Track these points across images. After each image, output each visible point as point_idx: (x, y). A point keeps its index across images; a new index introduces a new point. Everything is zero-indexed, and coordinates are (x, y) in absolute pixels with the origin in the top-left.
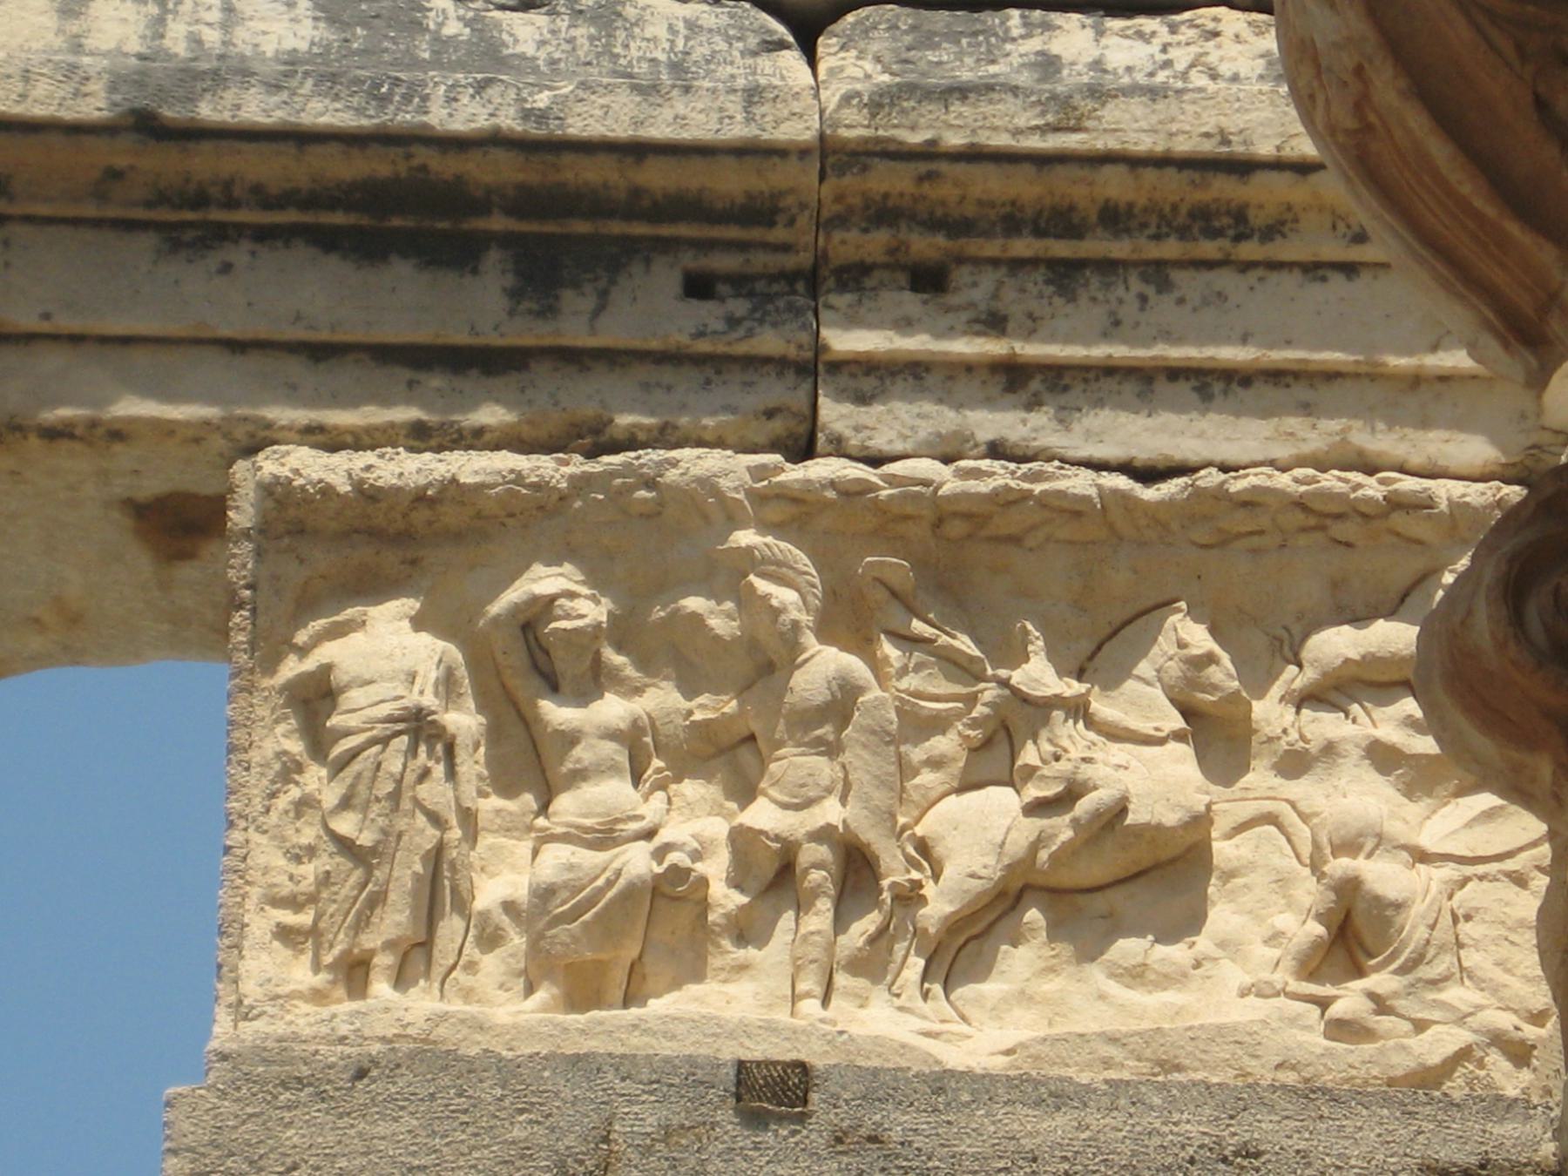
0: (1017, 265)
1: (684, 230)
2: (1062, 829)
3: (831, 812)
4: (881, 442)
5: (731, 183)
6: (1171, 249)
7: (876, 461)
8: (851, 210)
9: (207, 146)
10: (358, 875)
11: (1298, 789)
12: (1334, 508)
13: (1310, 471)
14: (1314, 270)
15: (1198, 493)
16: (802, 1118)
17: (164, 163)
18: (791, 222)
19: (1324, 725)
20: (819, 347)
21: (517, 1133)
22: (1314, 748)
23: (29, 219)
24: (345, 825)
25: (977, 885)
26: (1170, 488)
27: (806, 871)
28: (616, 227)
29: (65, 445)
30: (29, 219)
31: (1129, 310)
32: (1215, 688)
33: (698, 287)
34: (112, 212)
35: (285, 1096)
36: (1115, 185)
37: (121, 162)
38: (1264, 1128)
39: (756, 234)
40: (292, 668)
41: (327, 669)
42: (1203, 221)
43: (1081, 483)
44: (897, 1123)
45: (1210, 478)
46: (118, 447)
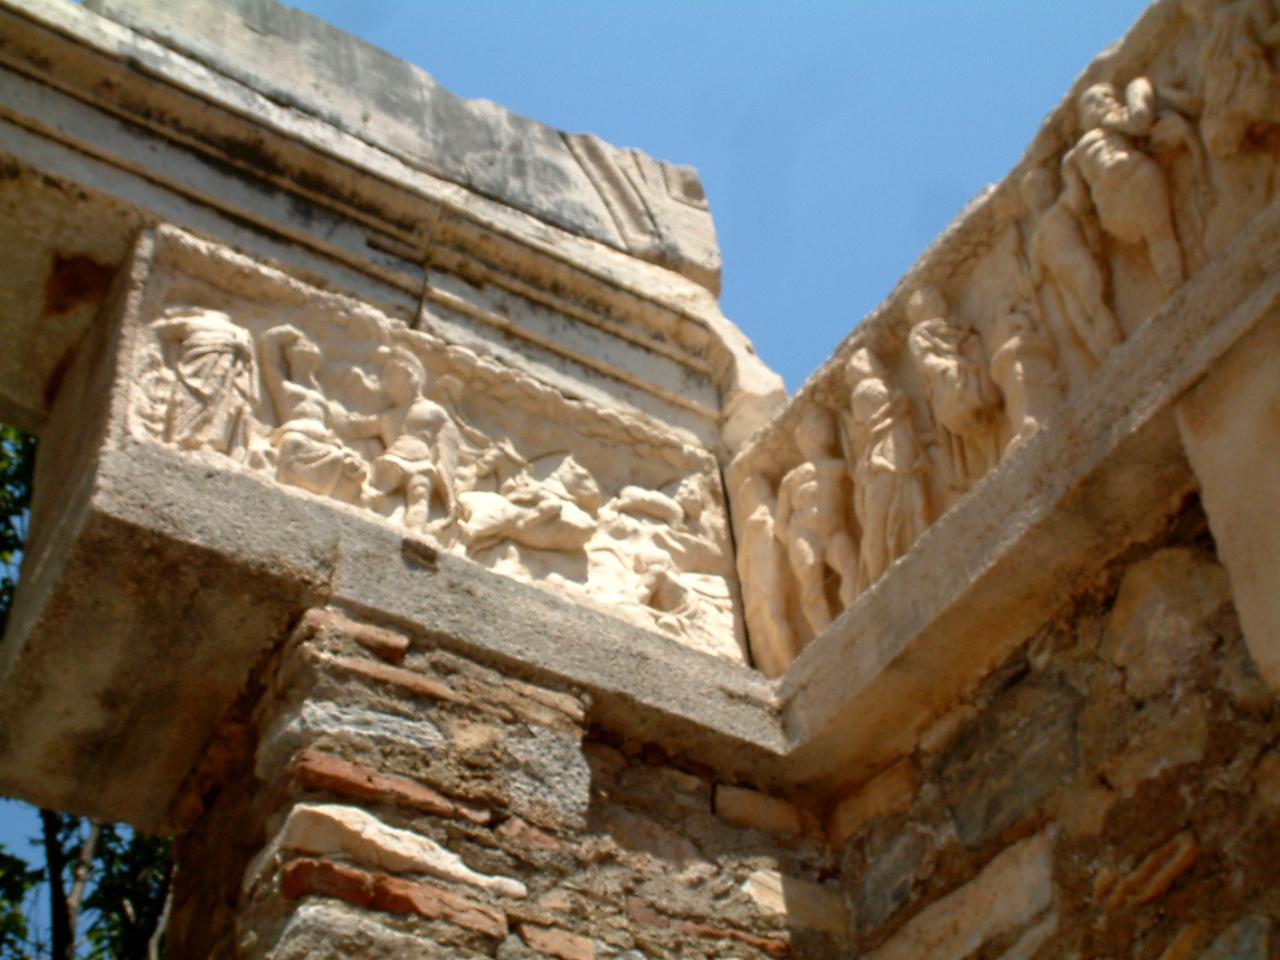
0: (514, 293)
3: (426, 465)
6: (577, 311)
9: (161, 87)
10: (198, 406)
12: (640, 436)
14: (633, 344)
17: (134, 86)
19: (630, 523)
20: (426, 289)
21: (290, 528)
23: (56, 89)
24: (195, 383)
25: (493, 522)
26: (574, 404)
27: (415, 487)
29: (53, 192)
30: (56, 89)
31: (559, 328)
32: (586, 489)
33: (373, 245)
34: (102, 102)
35: (167, 472)
36: (563, 275)
37: (115, 78)
38: (650, 649)
39: (402, 234)
40: (161, 322)
41: (183, 326)
42: (593, 305)
46: (81, 205)
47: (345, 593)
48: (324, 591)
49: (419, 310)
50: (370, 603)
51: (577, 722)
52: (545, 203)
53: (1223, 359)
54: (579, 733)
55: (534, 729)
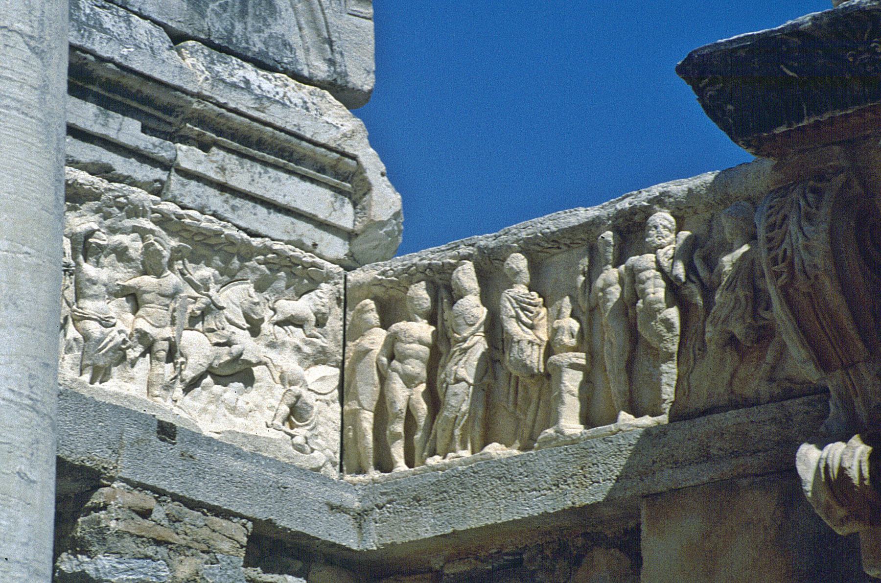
1: (146, 109)
2: (225, 355)
4: (187, 201)
5: (165, 98)
7: (183, 208)
8: (193, 118)
11: (272, 354)
13: (292, 247)
15: (265, 247)
16: (174, 444)
18: (177, 116)
22: (279, 341)
26: (256, 242)
28: (129, 102)
38: (289, 480)
43: (234, 232)
44: (199, 453)
45: (268, 242)
47: (125, 474)
48: (113, 473)
49: (169, 177)
50: (137, 479)
51: (242, 547)
52: (257, 44)
53: (675, 491)
54: (243, 553)
55: (219, 556)
